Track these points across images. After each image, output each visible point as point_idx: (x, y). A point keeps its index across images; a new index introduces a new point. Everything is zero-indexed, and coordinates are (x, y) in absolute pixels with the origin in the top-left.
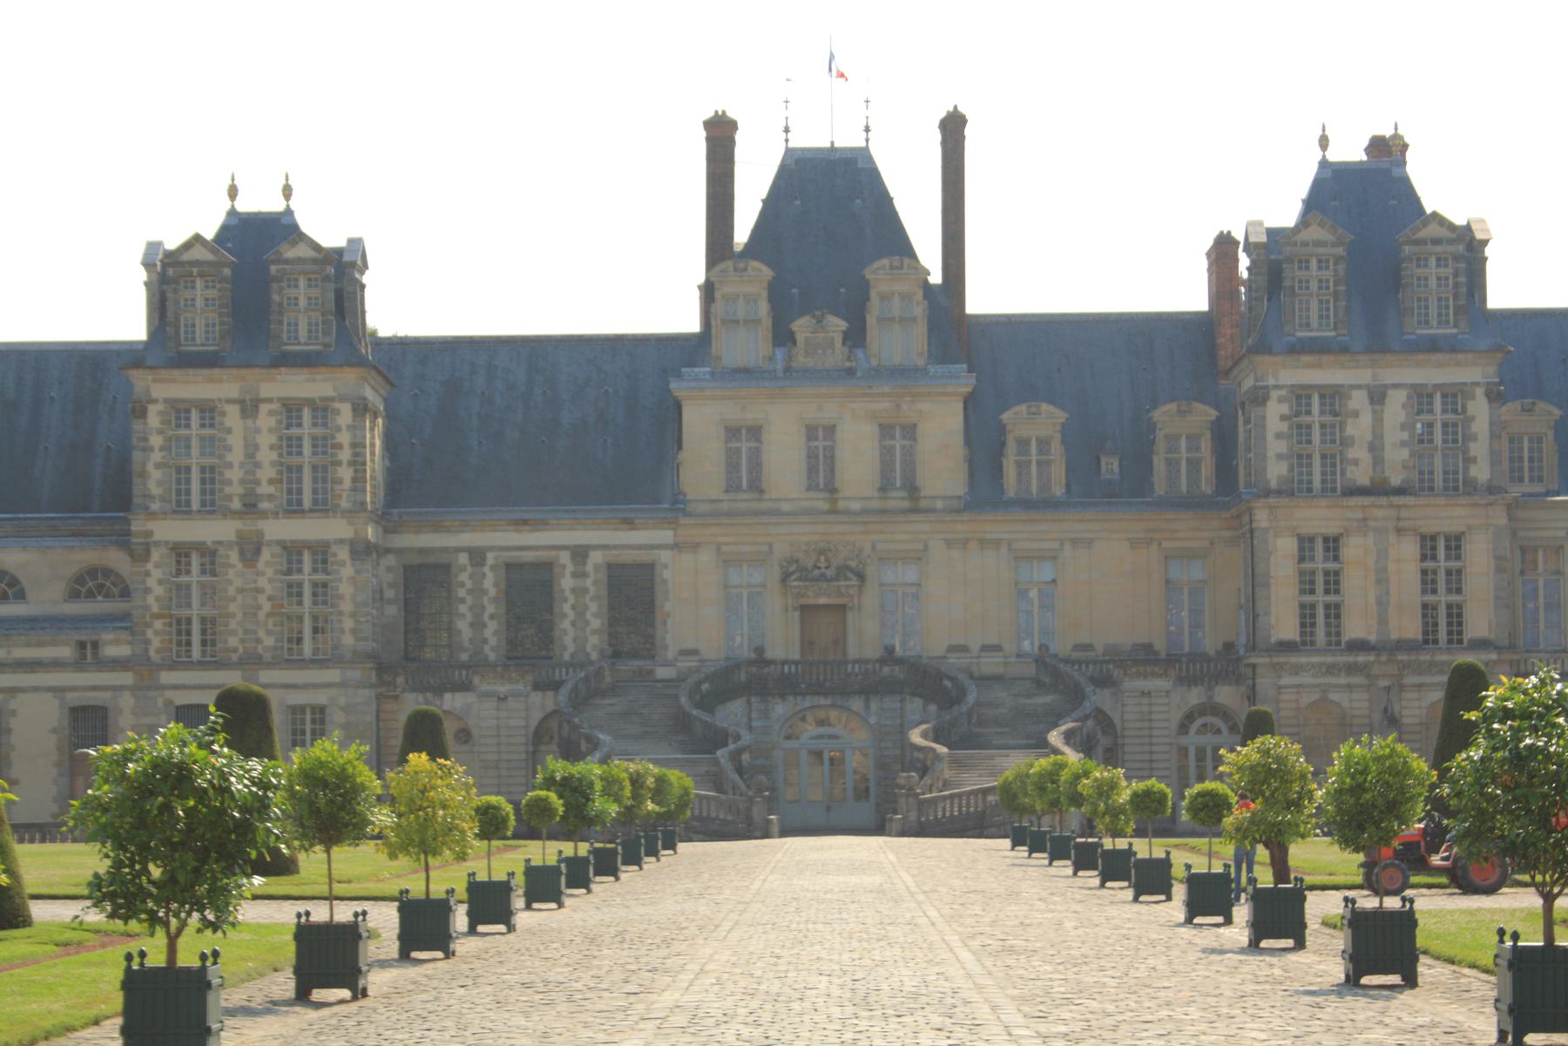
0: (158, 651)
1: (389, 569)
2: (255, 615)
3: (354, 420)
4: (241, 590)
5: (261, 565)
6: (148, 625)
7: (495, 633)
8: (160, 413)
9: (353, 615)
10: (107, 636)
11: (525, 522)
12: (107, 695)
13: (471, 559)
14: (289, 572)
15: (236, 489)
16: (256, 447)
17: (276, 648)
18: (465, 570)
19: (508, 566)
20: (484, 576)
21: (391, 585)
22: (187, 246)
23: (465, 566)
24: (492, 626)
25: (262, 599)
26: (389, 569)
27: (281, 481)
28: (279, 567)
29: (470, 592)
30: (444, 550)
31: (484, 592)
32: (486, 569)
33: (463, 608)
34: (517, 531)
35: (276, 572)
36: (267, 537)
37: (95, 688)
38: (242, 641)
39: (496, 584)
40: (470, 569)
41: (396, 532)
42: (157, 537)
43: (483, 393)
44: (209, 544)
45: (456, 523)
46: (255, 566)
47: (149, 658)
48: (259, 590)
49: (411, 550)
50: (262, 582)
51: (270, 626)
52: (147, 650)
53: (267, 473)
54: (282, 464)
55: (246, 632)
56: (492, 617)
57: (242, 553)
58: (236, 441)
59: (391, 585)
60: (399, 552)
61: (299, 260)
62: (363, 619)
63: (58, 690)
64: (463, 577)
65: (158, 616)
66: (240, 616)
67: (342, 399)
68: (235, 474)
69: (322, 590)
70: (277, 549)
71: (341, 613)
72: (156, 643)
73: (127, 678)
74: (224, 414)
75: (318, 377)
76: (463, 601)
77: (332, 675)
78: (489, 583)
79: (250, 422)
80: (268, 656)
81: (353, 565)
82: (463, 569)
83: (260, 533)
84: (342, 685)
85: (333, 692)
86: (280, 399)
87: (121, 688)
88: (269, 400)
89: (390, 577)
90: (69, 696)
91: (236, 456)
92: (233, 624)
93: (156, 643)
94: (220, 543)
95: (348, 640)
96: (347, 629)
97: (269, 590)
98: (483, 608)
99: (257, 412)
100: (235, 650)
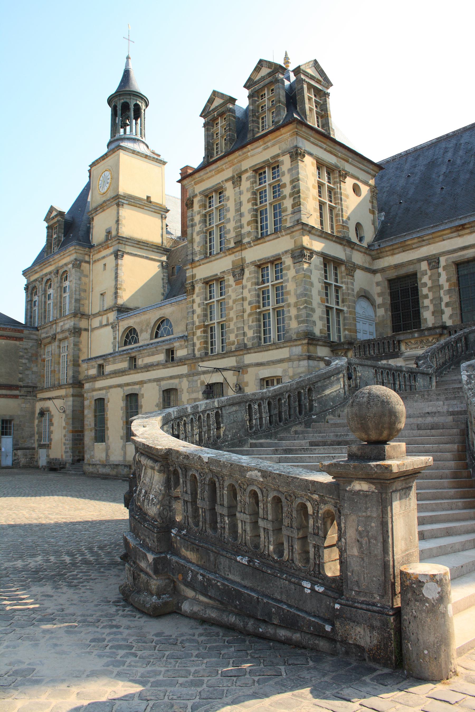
0: (199, 350)
1: (378, 284)
2: (242, 316)
3: (291, 165)
4: (234, 301)
5: (244, 281)
6: (194, 334)
7: (451, 317)
8: (199, 201)
9: (296, 305)
10: (176, 344)
11: (463, 227)
12: (176, 381)
13: (429, 264)
14: (263, 282)
15: (232, 234)
16: (241, 203)
17: (253, 338)
18: (426, 274)
19: (458, 265)
20: (439, 275)
21: (379, 295)
22: (211, 101)
23: (426, 270)
24: (448, 311)
25: (246, 304)
26: (378, 284)
27: (257, 222)
28: (254, 280)
29: (430, 289)
30: (411, 262)
31: (440, 287)
32: (441, 270)
33: (426, 302)
34: (459, 236)
35: (252, 284)
36: (248, 261)
37: (171, 378)
38: (237, 336)
39: (448, 280)
40: (429, 272)
41: (380, 258)
42: (198, 277)
43: (449, 161)
44: (219, 274)
45: (416, 241)
46: (242, 283)
47: (194, 355)
48: (243, 299)
49: (389, 267)
50: (246, 293)
51: (250, 323)
52: (194, 350)
53: (247, 217)
54: (256, 210)
55: (238, 329)
56: (447, 305)
57: (234, 276)
58: (231, 205)
59: (379, 295)
60: (383, 270)
61: (263, 78)
62: (301, 307)
63: (158, 380)
64: (425, 279)
65: (198, 327)
66: (235, 320)
67: (283, 154)
68: (231, 226)
69: (279, 289)
70: (252, 268)
71: (289, 305)
72: (198, 346)
73: (183, 370)
74: (226, 189)
75: (269, 144)
76: (426, 297)
77: (284, 353)
78: (443, 280)
79: (237, 189)
80: (249, 345)
81: (294, 267)
82: (425, 273)
83: (243, 259)
84: (289, 360)
85: (285, 365)
86: (250, 168)
87: (179, 377)
88: (246, 171)
89: (378, 289)
90: (163, 383)
91: (231, 214)
92: (232, 326)
93: (198, 346)
94: (224, 272)
95: (294, 325)
96: (293, 317)
97: (249, 299)
98: (441, 299)
99: (241, 181)
100: (233, 343)
